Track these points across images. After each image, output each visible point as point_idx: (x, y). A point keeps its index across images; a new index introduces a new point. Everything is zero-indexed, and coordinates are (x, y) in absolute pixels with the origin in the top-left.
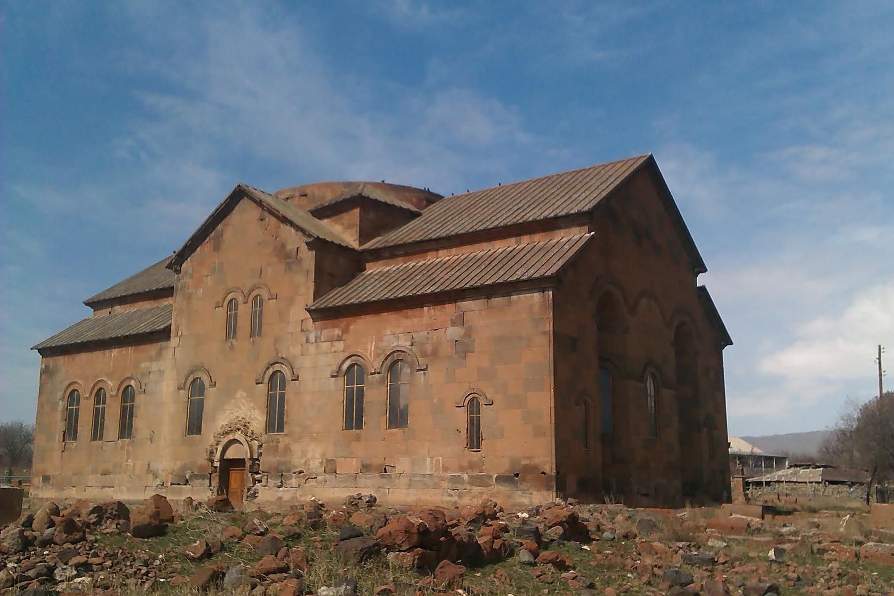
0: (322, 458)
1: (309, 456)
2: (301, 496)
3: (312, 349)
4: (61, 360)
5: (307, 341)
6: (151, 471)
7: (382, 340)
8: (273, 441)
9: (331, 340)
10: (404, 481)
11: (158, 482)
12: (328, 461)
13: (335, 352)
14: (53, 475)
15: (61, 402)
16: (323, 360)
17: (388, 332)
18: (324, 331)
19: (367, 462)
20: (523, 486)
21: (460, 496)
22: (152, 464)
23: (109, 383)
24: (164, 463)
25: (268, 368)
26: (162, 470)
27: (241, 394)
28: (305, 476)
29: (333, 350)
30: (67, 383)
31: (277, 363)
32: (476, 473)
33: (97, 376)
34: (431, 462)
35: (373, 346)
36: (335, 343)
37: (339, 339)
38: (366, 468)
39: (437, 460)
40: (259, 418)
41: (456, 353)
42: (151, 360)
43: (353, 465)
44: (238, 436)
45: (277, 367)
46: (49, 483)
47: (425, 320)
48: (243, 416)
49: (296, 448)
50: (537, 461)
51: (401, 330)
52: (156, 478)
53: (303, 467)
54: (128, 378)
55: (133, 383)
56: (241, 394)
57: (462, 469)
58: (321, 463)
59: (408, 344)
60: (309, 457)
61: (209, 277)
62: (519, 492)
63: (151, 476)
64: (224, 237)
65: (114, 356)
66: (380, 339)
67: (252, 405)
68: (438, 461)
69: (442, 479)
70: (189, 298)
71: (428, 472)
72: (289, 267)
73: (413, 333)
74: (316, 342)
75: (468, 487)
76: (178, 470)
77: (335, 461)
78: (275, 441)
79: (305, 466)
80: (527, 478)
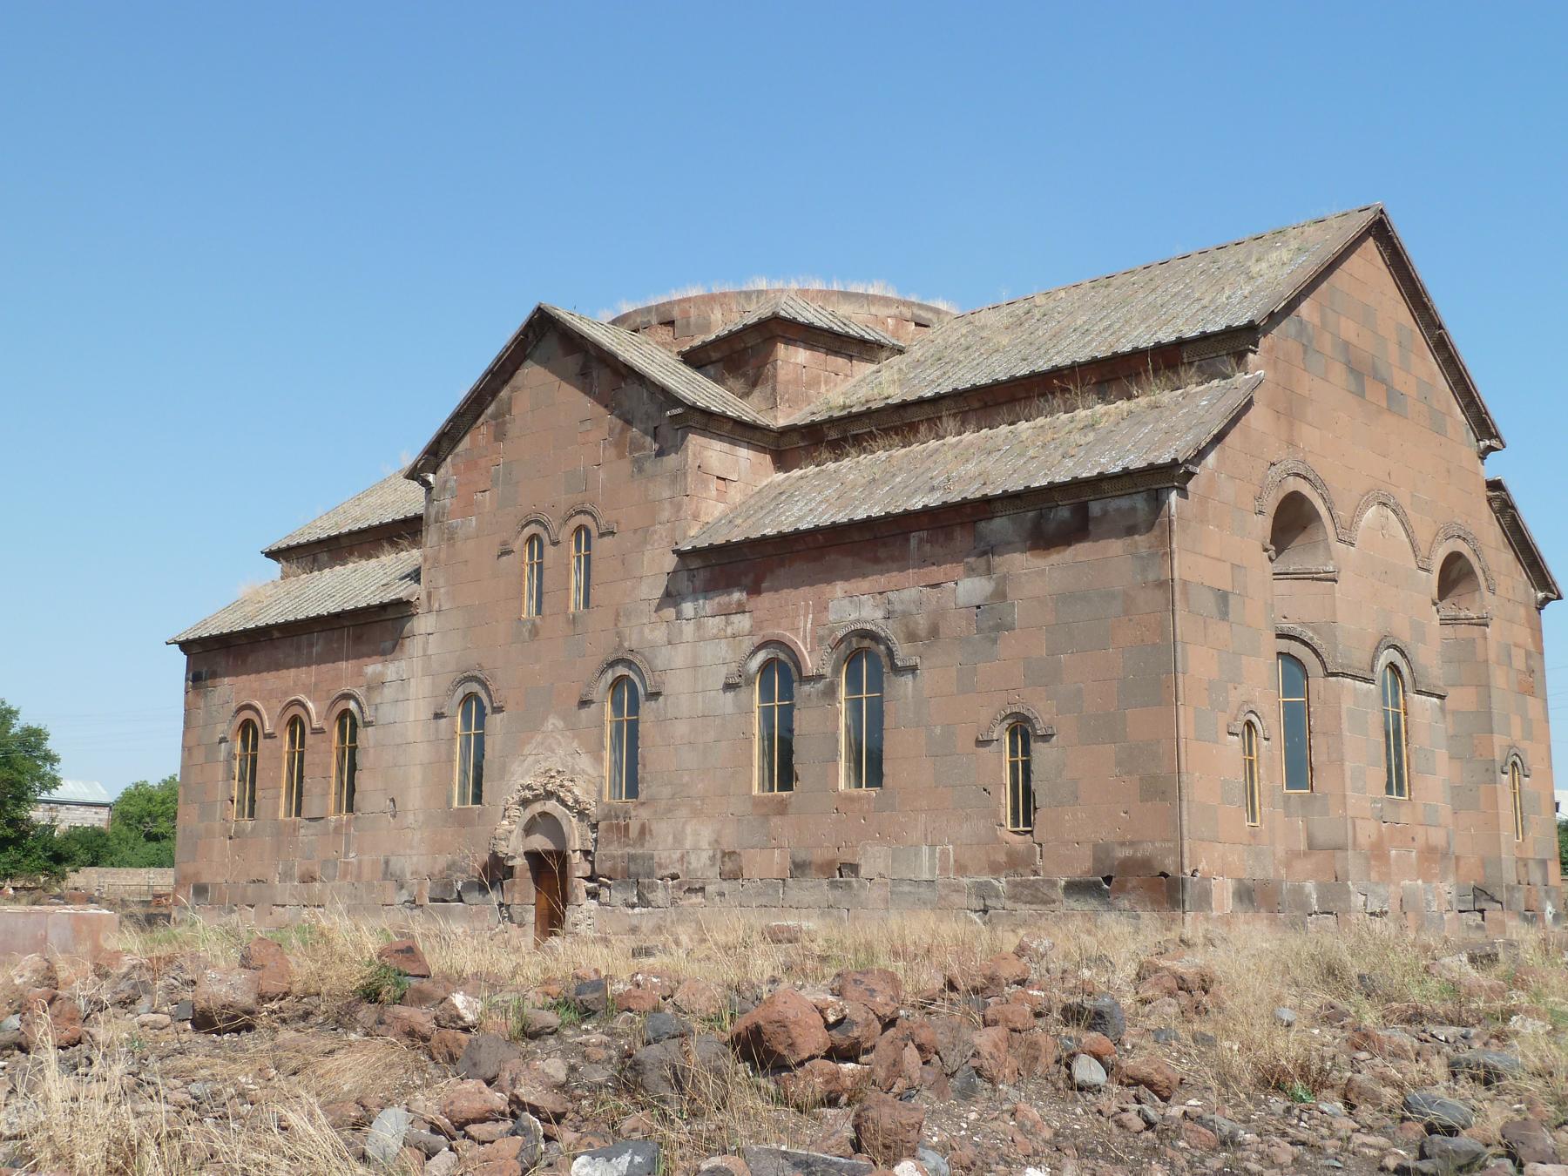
0: (715, 850)
7: (826, 609)
8: (617, 817)
11: (404, 895)
12: (724, 854)
13: (734, 636)
19: (802, 855)
22: (393, 859)
23: (310, 705)
24: (415, 859)
25: (603, 672)
27: (553, 724)
28: (680, 886)
29: (729, 631)
33: (286, 694)
34: (932, 855)
35: (810, 621)
36: (736, 618)
38: (799, 868)
39: (945, 853)
41: (979, 630)
43: (778, 860)
49: (663, 830)
50: (1146, 850)
52: (402, 887)
53: (678, 866)
56: (553, 724)
57: (995, 869)
58: (713, 858)
59: (879, 614)
60: (688, 847)
62: (1114, 915)
63: (390, 885)
67: (575, 745)
68: (945, 853)
69: (957, 889)
71: (926, 876)
73: (892, 596)
75: (1009, 904)
77: (739, 855)
78: (622, 815)
79: (682, 865)
80: (1129, 885)
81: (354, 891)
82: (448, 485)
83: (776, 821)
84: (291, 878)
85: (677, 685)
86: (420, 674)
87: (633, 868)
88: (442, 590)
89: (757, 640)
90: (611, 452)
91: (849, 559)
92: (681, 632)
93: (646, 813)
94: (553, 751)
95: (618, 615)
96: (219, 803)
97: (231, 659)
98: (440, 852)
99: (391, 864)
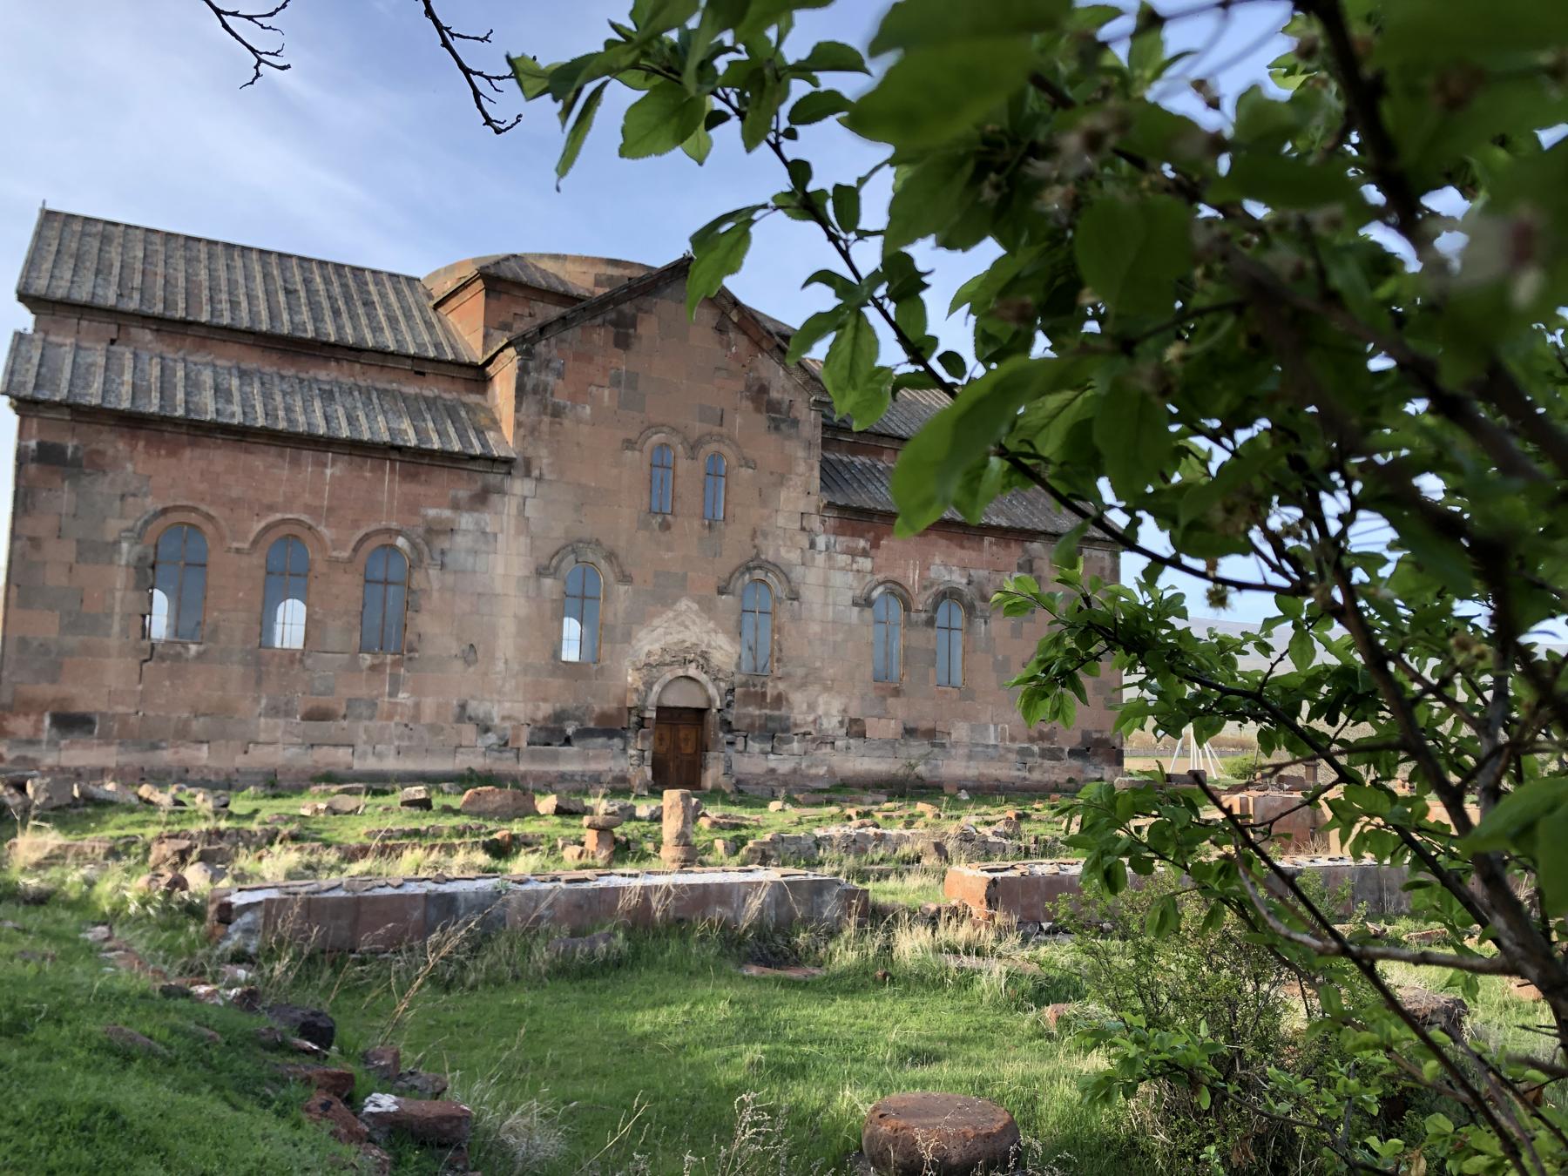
1: (820, 711)
2: (809, 767)
3: (820, 559)
4: (114, 445)
5: (813, 545)
6: (470, 718)
9: (853, 553)
10: (962, 751)
14: (103, 715)
15: (125, 546)
16: (838, 579)
17: (937, 560)
18: (841, 539)
19: (911, 725)
20: (1097, 760)
21: (1030, 770)
23: (322, 529)
25: (743, 574)
26: (504, 718)
28: (814, 740)
29: (855, 567)
30: (152, 504)
31: (760, 568)
32: (1046, 745)
33: (271, 508)
36: (860, 560)
37: (865, 554)
38: (910, 732)
40: (727, 647)
42: (456, 506)
43: (891, 728)
44: (692, 671)
45: (759, 574)
46: (91, 732)
47: (986, 556)
48: (694, 640)
49: (798, 699)
50: (1107, 735)
51: (955, 561)
54: (388, 531)
55: (401, 542)
57: (1032, 740)
58: (841, 723)
59: (964, 581)
61: (606, 392)
63: (469, 731)
64: (641, 330)
65: (332, 475)
66: (926, 567)
67: (711, 625)
69: (1009, 750)
70: (557, 412)
71: (992, 742)
72: (776, 426)
74: (827, 548)
76: (546, 719)
81: (407, 731)
82: (553, 365)
83: (891, 701)
84: (288, 714)
85: (812, 595)
86: (512, 532)
87: (771, 725)
88: (545, 461)
89: (880, 577)
90: (747, 405)
91: (943, 542)
92: (813, 559)
93: (781, 686)
94: (687, 627)
95: (755, 532)
96: (117, 618)
97: (141, 444)
98: (545, 700)
99: (470, 711)
